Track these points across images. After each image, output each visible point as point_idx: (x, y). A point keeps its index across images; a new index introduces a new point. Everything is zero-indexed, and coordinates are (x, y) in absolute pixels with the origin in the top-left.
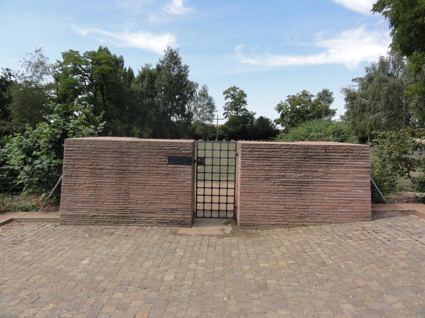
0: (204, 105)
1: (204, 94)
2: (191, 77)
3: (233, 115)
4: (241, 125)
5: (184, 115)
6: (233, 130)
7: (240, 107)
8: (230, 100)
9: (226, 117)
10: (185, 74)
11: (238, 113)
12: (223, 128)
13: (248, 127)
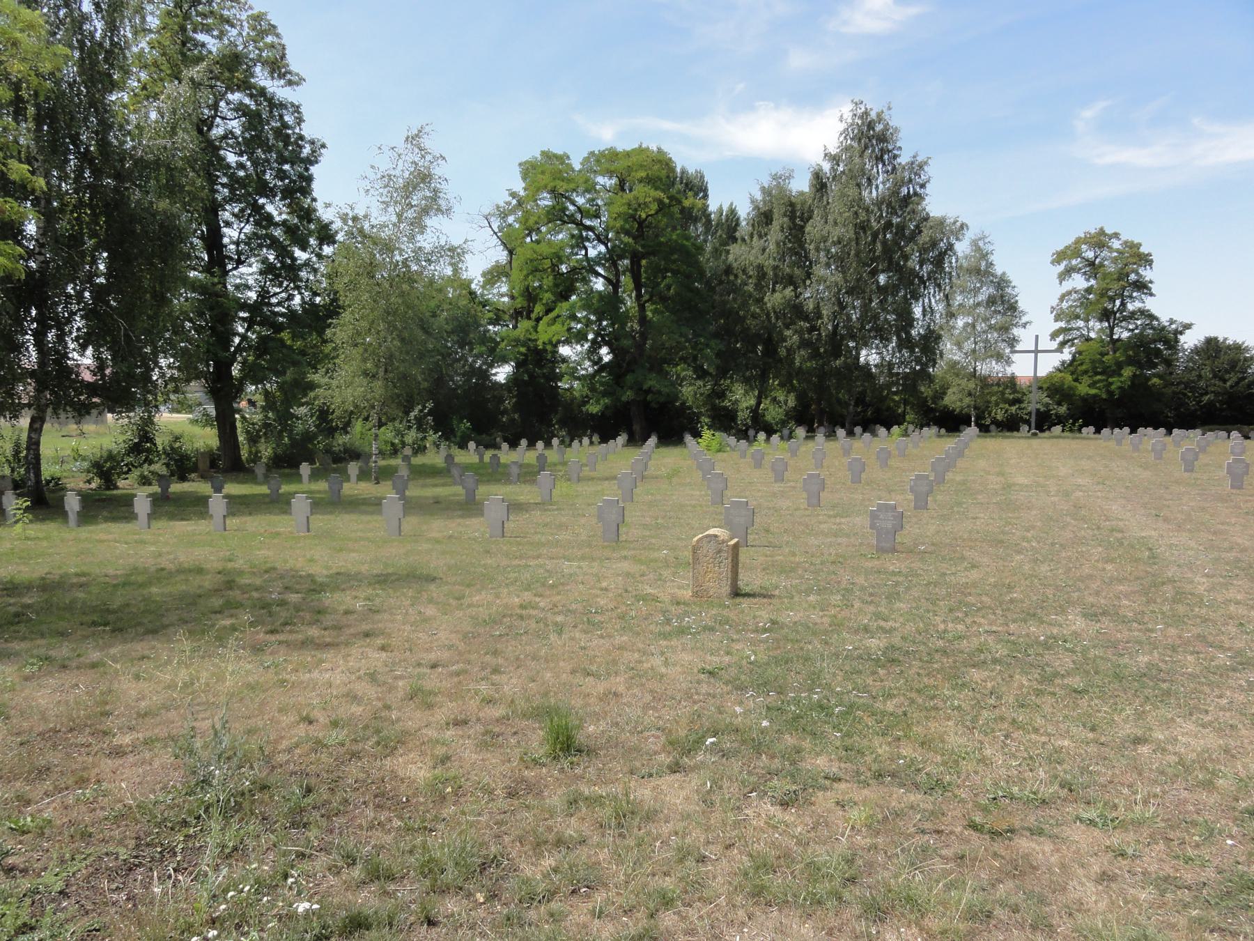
0: (979, 304)
1: (981, 270)
2: (936, 205)
3: (1093, 335)
4: (1127, 372)
5: (906, 343)
6: (1093, 391)
7: (1123, 304)
8: (1079, 282)
9: (1063, 344)
10: (916, 194)
11: (1112, 329)
13: (1155, 380)
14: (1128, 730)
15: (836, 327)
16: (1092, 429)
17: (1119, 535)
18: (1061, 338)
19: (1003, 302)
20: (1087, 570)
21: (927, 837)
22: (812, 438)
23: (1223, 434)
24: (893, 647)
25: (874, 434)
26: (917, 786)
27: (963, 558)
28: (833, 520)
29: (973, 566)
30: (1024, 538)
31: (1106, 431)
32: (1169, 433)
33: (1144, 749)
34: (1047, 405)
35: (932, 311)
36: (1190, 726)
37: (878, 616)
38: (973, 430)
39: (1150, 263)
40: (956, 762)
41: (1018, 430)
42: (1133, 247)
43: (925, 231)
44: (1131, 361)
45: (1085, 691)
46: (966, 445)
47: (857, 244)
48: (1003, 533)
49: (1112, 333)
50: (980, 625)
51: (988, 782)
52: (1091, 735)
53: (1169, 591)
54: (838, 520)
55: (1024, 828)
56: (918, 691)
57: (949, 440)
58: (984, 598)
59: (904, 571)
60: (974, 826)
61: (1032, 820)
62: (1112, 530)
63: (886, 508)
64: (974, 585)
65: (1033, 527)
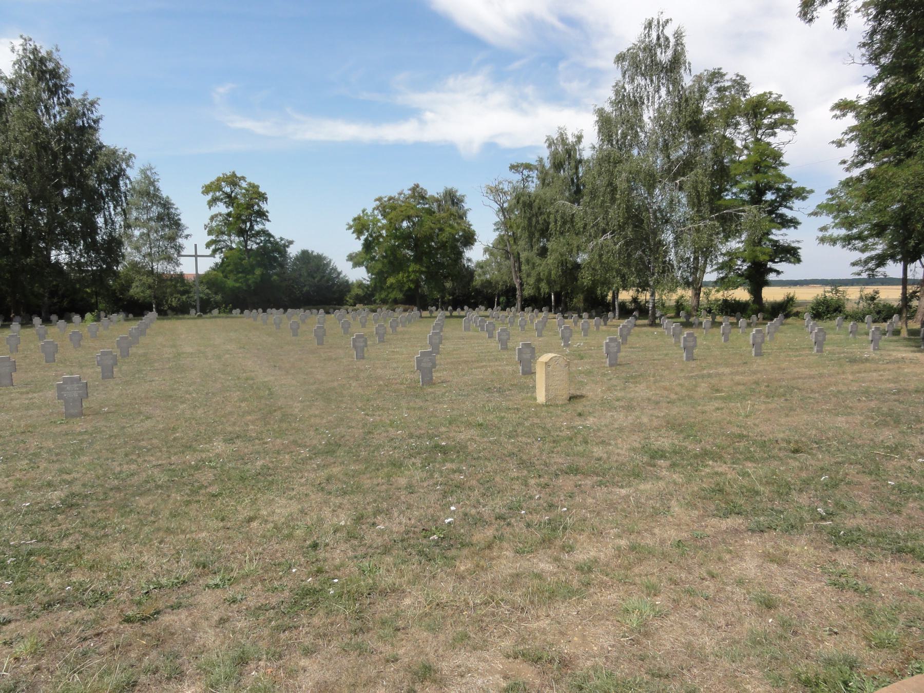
0: (150, 219)
1: (149, 192)
2: (108, 136)
3: (234, 246)
4: (258, 272)
5: (92, 246)
6: (237, 285)
7: (252, 226)
8: (222, 208)
9: (215, 251)
10: (90, 127)
11: (246, 242)
12: (208, 280)
13: (275, 277)
14: (247, 513)
15: (24, 230)
16: (238, 310)
17: (251, 382)
18: (213, 247)
19: (169, 218)
20: (229, 409)
21: (88, 642)
22: (8, 326)
23: (315, 311)
24: (73, 495)
25: (69, 320)
26: (83, 604)
27: (140, 413)
28: (25, 396)
29: (148, 418)
30: (187, 392)
31: (246, 311)
32: (285, 310)
33: (254, 524)
34: (207, 294)
35: (113, 223)
36: (283, 501)
37: (62, 471)
38: (153, 315)
39: (266, 199)
40: (119, 574)
41: (188, 313)
42: (254, 187)
43: (101, 158)
44: (260, 265)
45: (220, 494)
46: (147, 326)
47: (39, 160)
48: (174, 390)
49: (246, 245)
50: (149, 462)
51: (143, 581)
52: (221, 524)
53: (278, 415)
54: (30, 396)
55: (167, 607)
56: (92, 526)
57: (134, 322)
58: (155, 441)
59: (90, 430)
60: (128, 620)
61: (174, 599)
62: (247, 379)
63: (72, 381)
64: (147, 432)
65: (194, 383)
